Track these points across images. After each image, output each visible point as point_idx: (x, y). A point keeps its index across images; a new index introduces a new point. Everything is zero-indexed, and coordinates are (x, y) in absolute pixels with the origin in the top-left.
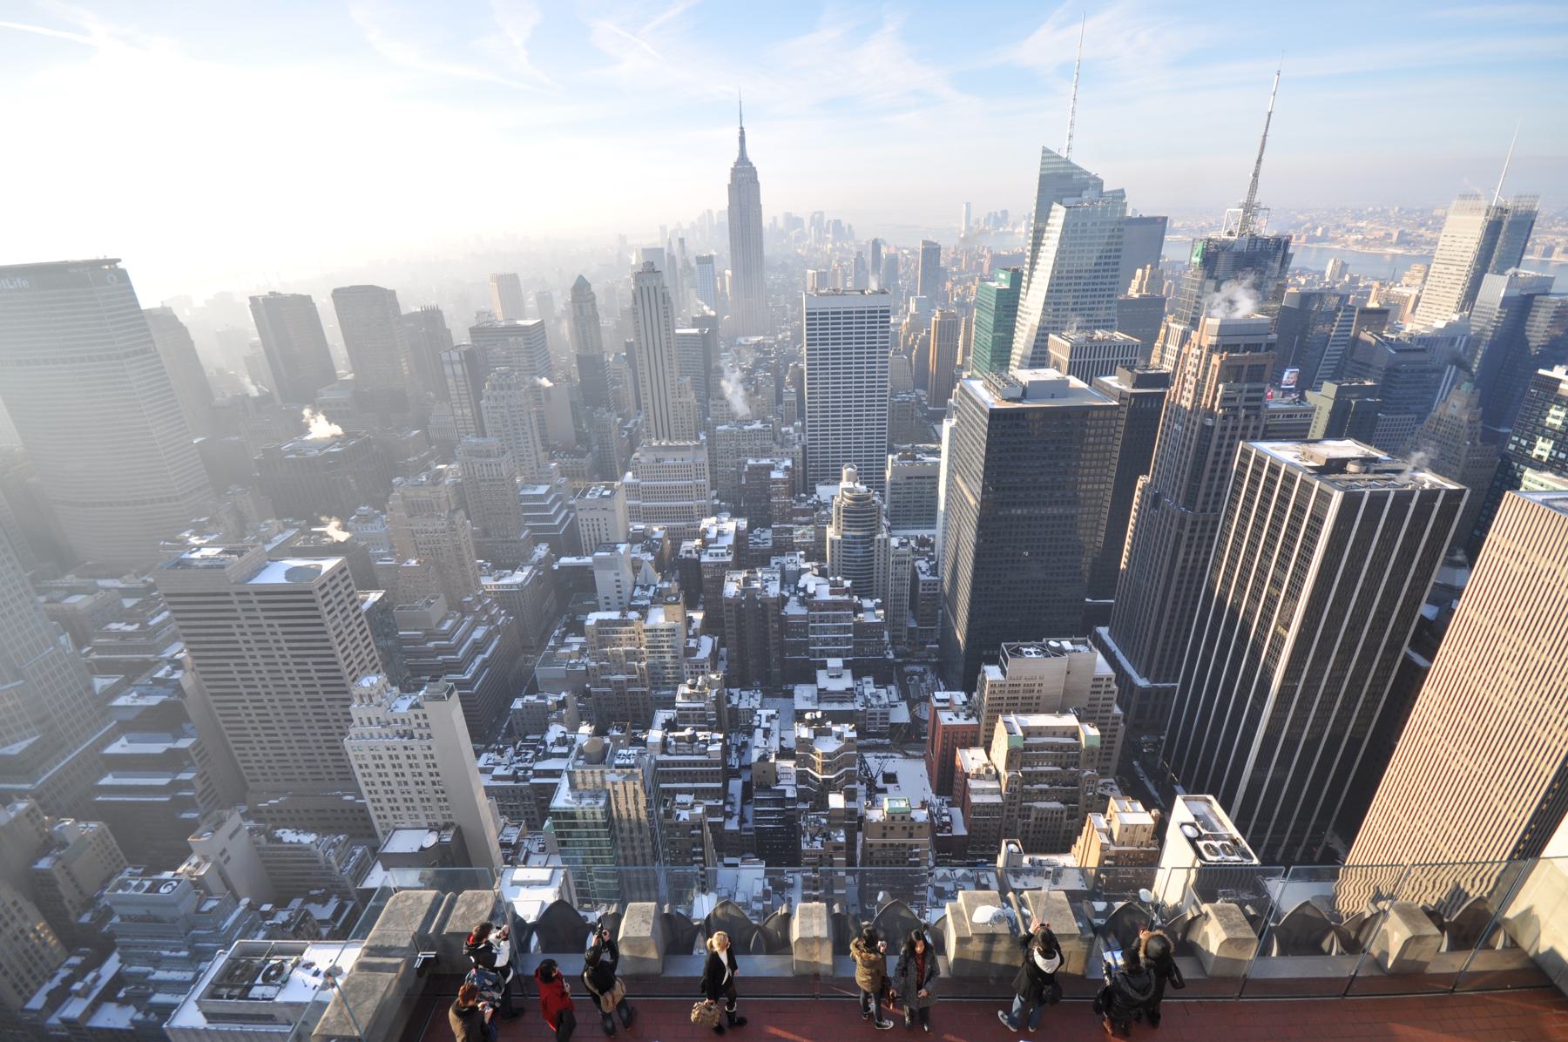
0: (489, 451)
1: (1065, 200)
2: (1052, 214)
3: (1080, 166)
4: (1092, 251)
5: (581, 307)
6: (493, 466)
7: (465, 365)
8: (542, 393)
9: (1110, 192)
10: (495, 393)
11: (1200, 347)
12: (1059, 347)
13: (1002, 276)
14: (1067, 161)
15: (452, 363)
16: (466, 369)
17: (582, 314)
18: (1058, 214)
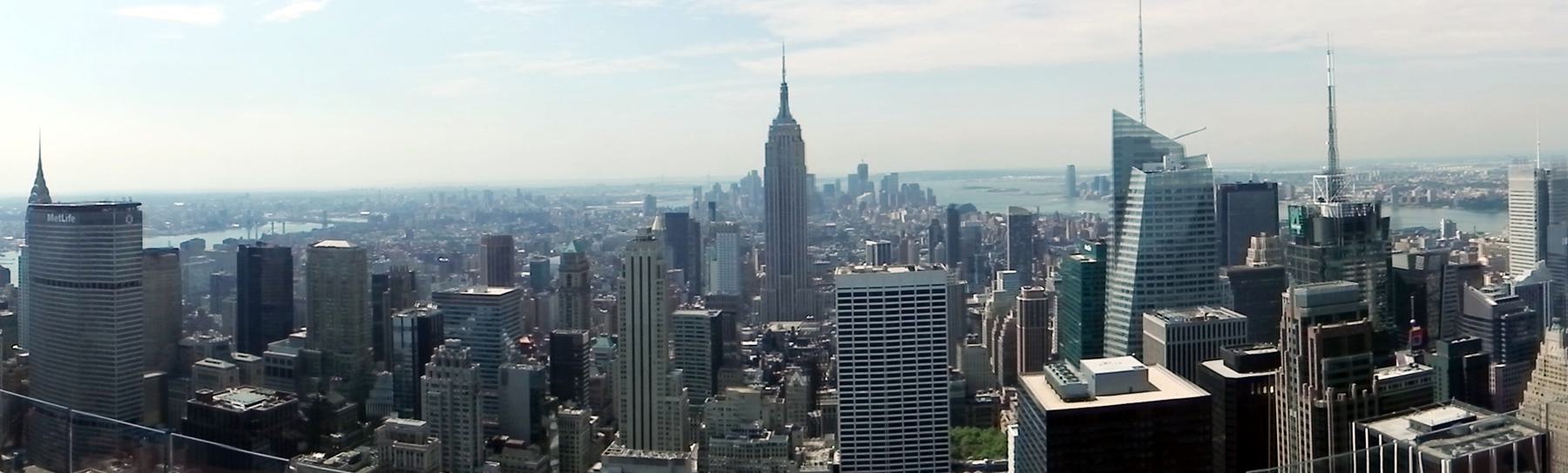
0: (413, 436)
1: (1147, 166)
2: (1132, 180)
3: (1157, 130)
4: (1180, 220)
5: (569, 277)
6: (415, 456)
7: (416, 333)
8: (499, 375)
9: (1191, 158)
10: (440, 369)
11: (1295, 321)
12: (1155, 326)
13: (1088, 248)
14: (1142, 126)
15: (402, 329)
16: (416, 337)
17: (569, 284)
18: (1138, 181)
